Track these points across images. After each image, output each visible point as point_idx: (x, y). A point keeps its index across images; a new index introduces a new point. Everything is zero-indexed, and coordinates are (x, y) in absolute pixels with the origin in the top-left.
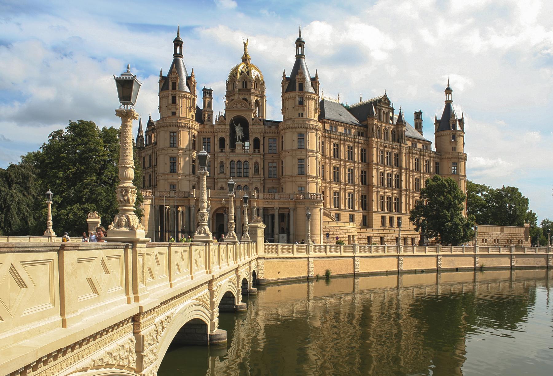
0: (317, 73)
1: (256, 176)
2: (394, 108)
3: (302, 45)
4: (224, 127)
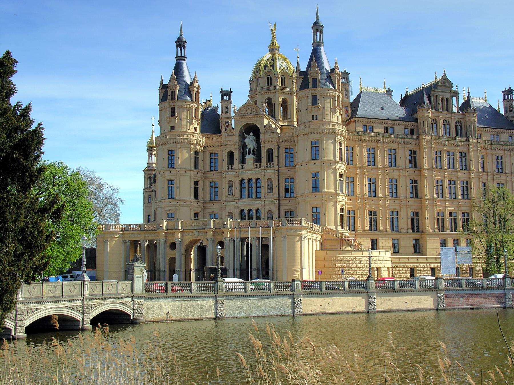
1: (270, 197)
2: (459, 91)
4: (232, 138)
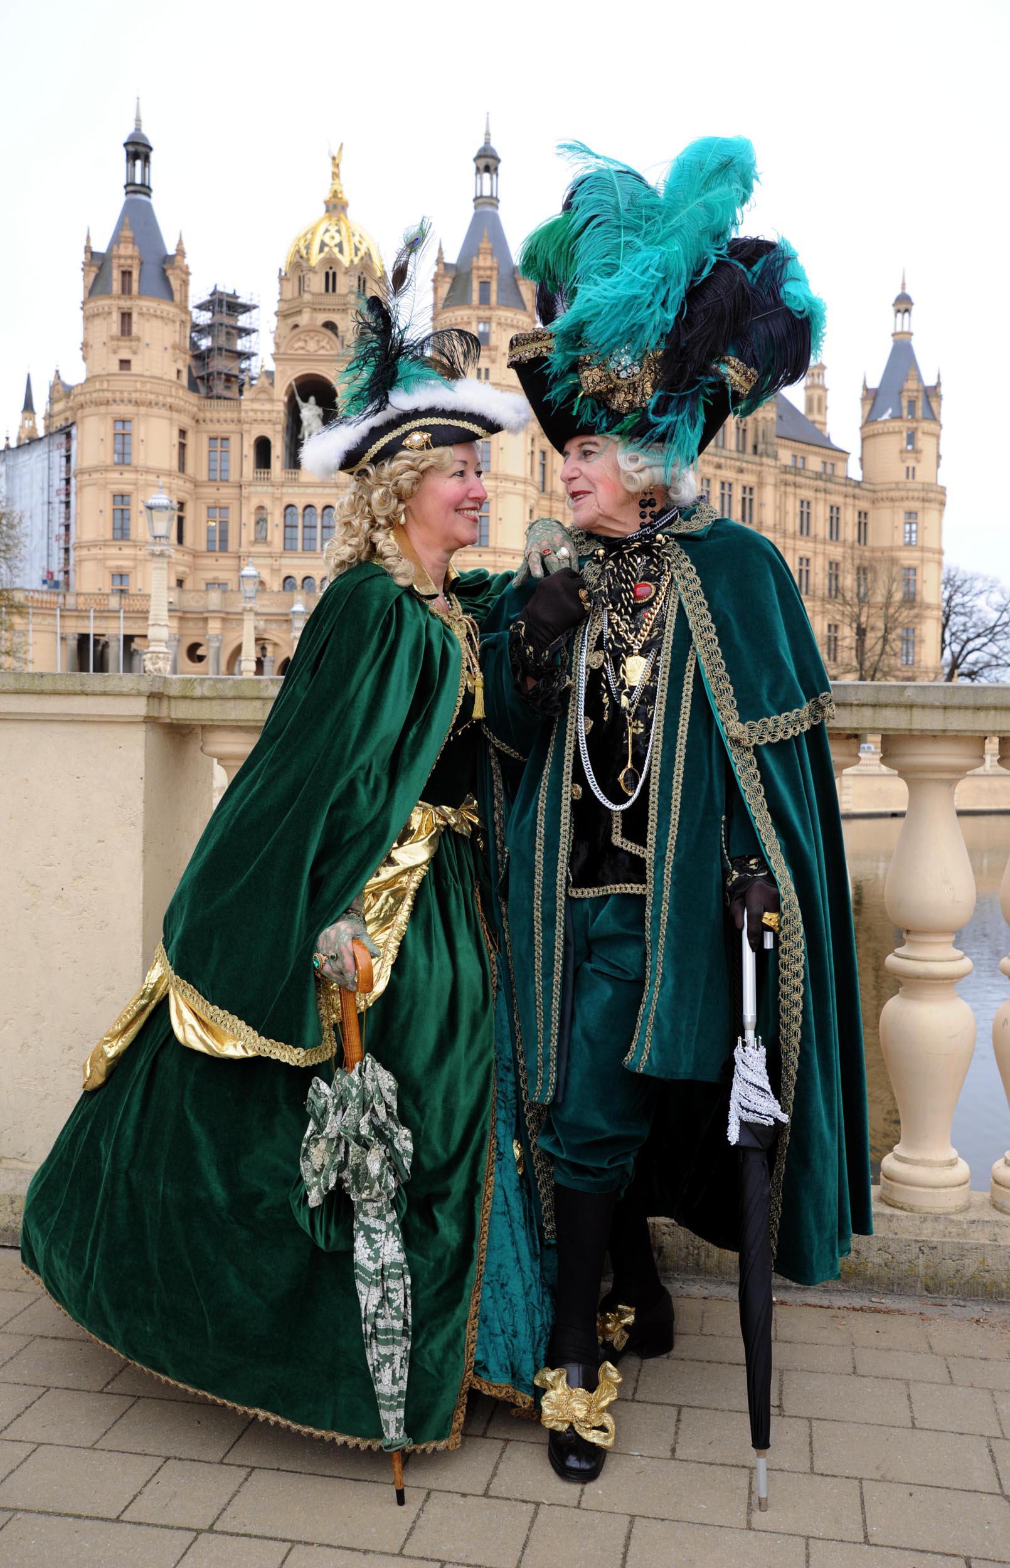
3: (492, 168)
4: (268, 407)
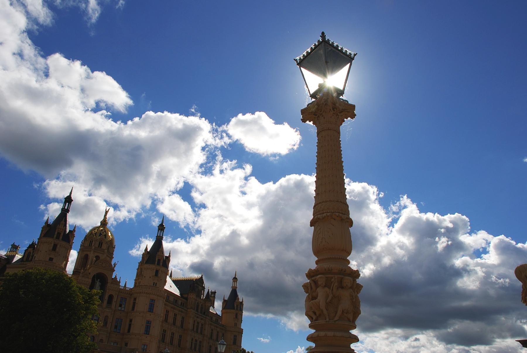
0: (170, 254)
